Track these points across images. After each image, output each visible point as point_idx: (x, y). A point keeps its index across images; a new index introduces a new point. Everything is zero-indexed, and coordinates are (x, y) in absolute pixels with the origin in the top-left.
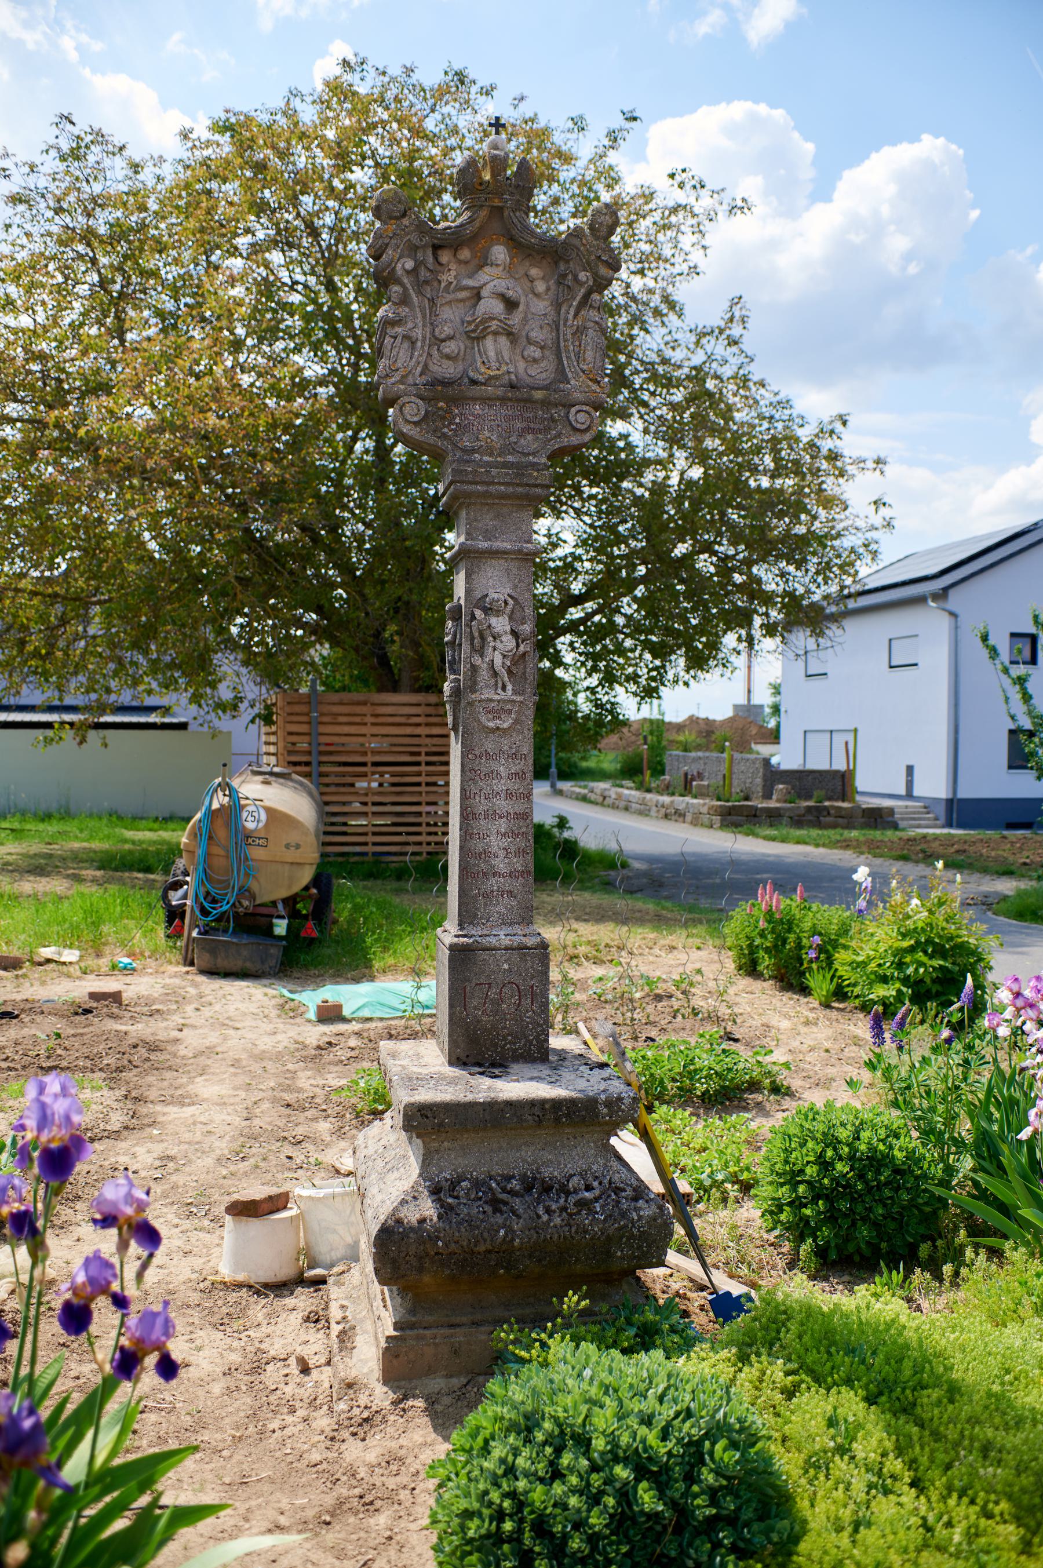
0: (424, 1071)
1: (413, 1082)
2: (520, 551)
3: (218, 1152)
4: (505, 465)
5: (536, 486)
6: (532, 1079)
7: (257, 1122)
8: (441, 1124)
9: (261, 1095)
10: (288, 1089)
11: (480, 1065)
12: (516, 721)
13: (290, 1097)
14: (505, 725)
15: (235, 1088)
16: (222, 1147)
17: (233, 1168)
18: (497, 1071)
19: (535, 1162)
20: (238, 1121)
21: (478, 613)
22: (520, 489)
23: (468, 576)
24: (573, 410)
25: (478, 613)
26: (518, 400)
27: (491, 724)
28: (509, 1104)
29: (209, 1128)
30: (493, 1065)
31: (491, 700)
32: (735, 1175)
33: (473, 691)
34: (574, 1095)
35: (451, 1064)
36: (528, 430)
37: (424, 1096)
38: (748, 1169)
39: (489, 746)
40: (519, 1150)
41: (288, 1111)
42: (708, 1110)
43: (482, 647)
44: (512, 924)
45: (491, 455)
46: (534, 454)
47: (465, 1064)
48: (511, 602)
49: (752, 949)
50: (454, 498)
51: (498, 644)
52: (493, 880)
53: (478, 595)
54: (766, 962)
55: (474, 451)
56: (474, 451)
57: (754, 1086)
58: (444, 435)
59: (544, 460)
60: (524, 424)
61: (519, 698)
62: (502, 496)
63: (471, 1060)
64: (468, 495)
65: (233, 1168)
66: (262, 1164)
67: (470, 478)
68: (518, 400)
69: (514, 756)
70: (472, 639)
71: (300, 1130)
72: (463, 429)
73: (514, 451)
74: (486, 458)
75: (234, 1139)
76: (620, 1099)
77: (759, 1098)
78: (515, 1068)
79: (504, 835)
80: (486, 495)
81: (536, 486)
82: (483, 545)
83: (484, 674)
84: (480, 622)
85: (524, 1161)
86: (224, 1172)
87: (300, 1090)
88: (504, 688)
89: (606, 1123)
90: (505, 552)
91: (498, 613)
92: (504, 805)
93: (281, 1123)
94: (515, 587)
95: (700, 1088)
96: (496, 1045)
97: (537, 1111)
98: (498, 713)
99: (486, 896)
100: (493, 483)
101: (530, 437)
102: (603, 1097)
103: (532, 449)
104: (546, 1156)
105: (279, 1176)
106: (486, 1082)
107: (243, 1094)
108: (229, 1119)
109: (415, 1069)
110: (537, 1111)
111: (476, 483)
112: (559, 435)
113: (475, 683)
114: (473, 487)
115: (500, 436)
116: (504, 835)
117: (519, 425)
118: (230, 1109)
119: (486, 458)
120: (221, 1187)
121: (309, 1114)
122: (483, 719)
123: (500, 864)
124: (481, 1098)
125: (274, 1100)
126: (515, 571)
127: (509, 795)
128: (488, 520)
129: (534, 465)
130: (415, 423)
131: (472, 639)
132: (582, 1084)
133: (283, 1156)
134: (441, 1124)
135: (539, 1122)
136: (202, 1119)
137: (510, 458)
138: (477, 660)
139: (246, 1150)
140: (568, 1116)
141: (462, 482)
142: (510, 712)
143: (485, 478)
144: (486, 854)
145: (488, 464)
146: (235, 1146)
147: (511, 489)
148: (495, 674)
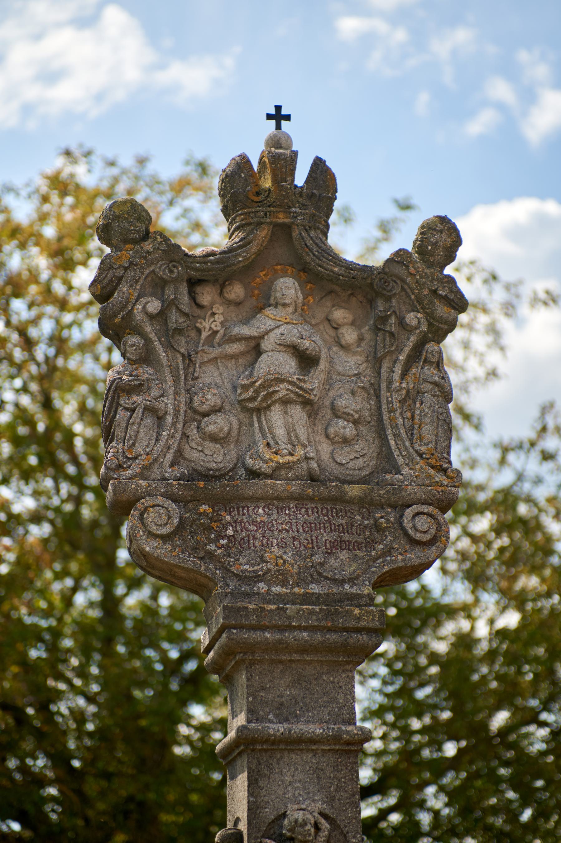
2: (337, 738)
4: (307, 599)
5: (358, 630)
22: (333, 637)
23: (252, 783)
24: (409, 512)
26: (323, 500)
36: (341, 544)
46: (352, 580)
48: (325, 825)
50: (227, 653)
53: (269, 814)
55: (256, 578)
56: (256, 578)
58: (210, 555)
59: (367, 590)
60: (334, 536)
62: (305, 649)
64: (250, 648)
67: (253, 620)
68: (323, 500)
72: (239, 544)
73: (319, 578)
74: (277, 589)
80: (279, 647)
81: (358, 630)
82: (277, 728)
90: (313, 741)
94: (330, 799)
100: (290, 628)
101: (344, 555)
103: (347, 573)
111: (264, 628)
112: (389, 551)
114: (257, 636)
115: (298, 554)
117: (325, 537)
119: (277, 589)
126: (329, 771)
128: (283, 688)
129: (352, 599)
130: (165, 538)
137: (314, 588)
141: (240, 627)
143: (277, 620)
145: (280, 598)
147: (318, 637)
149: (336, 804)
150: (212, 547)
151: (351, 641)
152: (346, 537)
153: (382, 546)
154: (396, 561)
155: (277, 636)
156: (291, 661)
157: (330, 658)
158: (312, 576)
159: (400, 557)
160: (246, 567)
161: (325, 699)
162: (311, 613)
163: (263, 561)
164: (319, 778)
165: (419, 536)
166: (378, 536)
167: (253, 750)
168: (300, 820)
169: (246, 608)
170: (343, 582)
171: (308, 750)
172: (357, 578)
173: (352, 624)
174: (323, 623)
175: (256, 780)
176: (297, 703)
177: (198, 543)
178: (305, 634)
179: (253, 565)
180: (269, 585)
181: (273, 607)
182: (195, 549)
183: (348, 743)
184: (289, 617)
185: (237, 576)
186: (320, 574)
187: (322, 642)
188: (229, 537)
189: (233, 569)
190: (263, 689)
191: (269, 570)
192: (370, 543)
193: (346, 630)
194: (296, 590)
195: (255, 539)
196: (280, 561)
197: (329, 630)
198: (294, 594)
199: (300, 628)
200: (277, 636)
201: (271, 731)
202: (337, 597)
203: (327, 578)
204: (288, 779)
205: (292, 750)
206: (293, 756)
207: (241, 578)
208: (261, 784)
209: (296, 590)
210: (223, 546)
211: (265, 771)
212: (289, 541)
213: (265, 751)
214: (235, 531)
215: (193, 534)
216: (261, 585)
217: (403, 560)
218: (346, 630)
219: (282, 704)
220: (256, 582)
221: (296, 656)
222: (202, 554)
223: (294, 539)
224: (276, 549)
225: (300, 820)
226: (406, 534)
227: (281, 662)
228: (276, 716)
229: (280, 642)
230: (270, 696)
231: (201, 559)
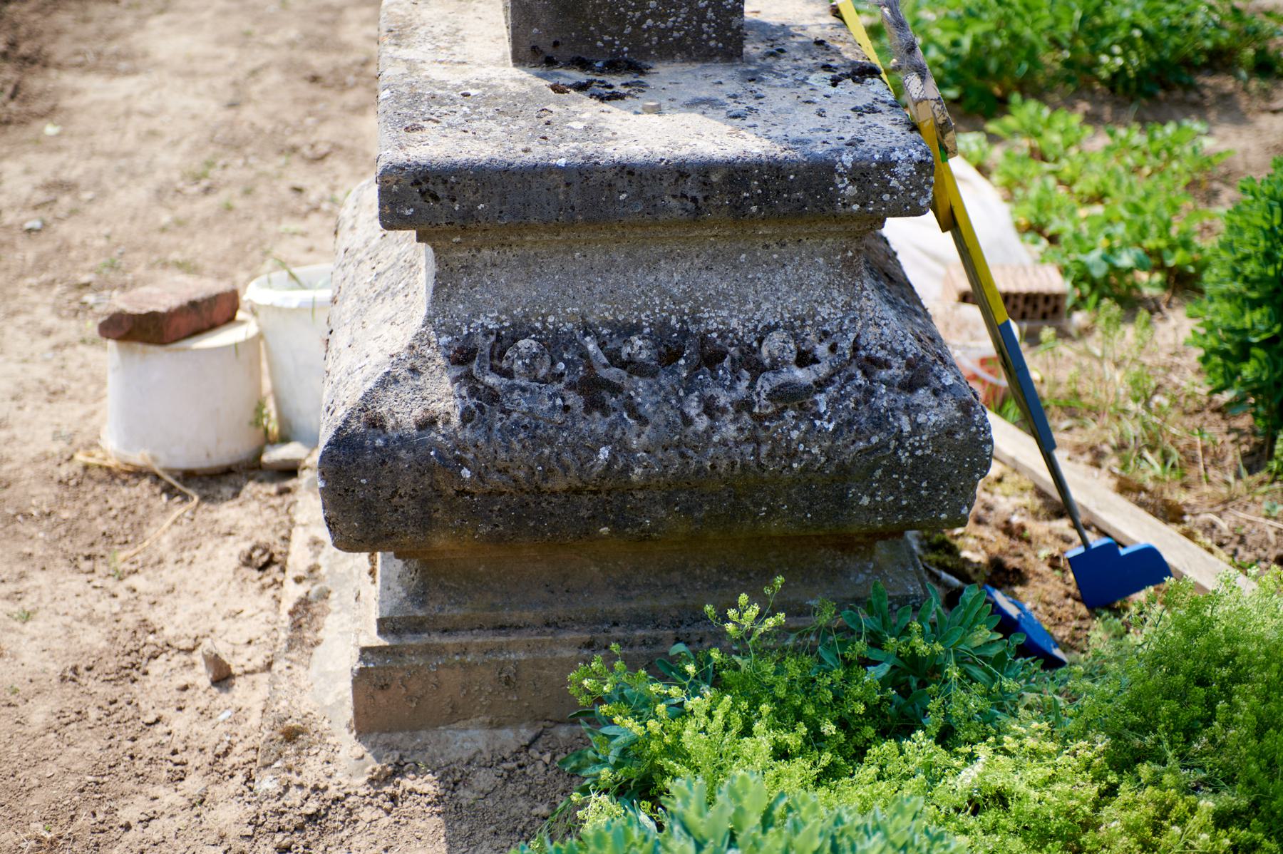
0: (454, 77)
1: (418, 106)
3: (160, 176)
6: (694, 104)
7: (248, 113)
8: (469, 215)
9: (264, 56)
10: (320, 44)
11: (582, 64)
13: (319, 62)
15: (221, 42)
16: (170, 162)
17: (183, 209)
18: (617, 82)
19: (688, 295)
20: (212, 110)
28: (627, 171)
29: (155, 124)
30: (614, 66)
32: (1156, 254)
34: (778, 151)
35: (519, 59)
37: (436, 147)
38: (1186, 245)
40: (652, 266)
41: (314, 91)
42: (1119, 106)
47: (550, 62)
57: (1220, 60)
63: (564, 52)
65: (183, 209)
66: (239, 203)
71: (327, 134)
75: (197, 148)
76: (887, 164)
77: (1229, 84)
78: (663, 73)
85: (664, 293)
86: (165, 218)
87: (343, 48)
89: (852, 217)
93: (291, 116)
95: (1110, 63)
96: (621, 20)
97: (691, 187)
102: (847, 159)
104: (716, 282)
105: (271, 228)
106: (587, 109)
107: (231, 54)
108: (196, 104)
109: (437, 73)
110: (691, 187)
118: (202, 85)
120: (154, 249)
121: (351, 98)
124: (561, 153)
125: (290, 68)
132: (804, 123)
133: (283, 188)
134: (469, 215)
135: (697, 214)
136: (145, 104)
139: (215, 173)
140: (762, 200)
146: (196, 165)
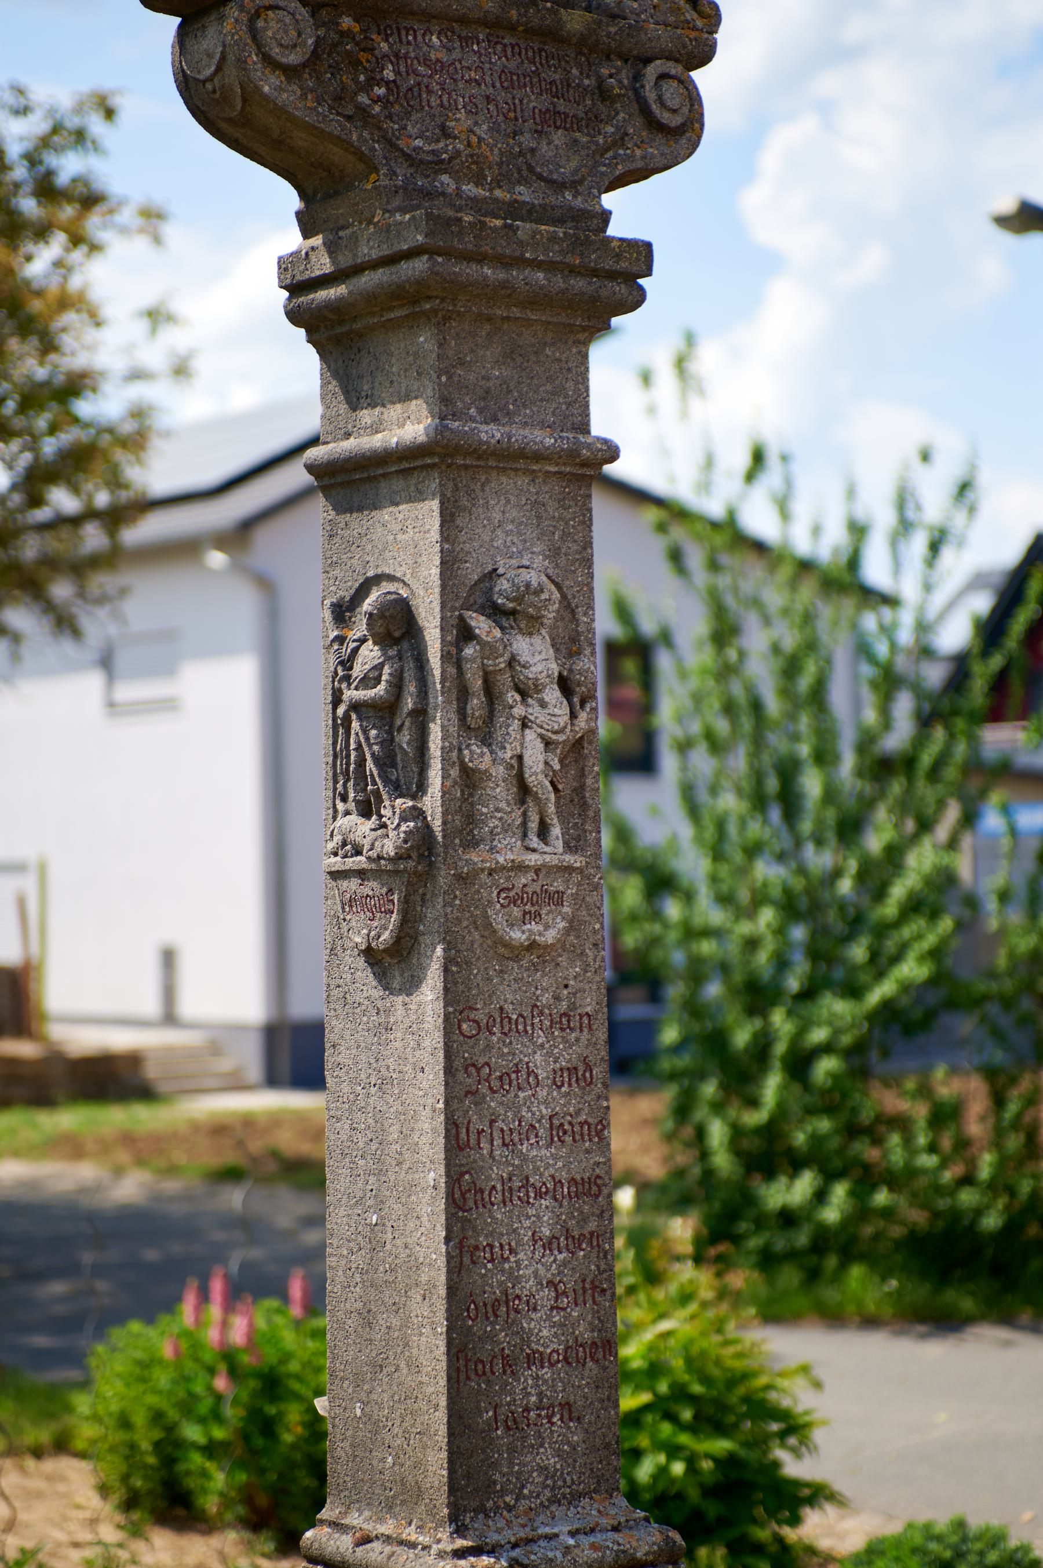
5: (612, 275)
12: (573, 926)
14: (550, 936)
21: (481, 624)
22: (579, 284)
24: (652, 71)
25: (481, 624)
26: (531, 32)
27: (517, 935)
31: (520, 868)
33: (472, 843)
36: (552, 119)
39: (509, 996)
43: (490, 718)
44: (575, 1498)
45: (479, 180)
49: (169, 1448)
51: (535, 712)
52: (528, 1375)
54: (216, 1483)
55: (438, 165)
56: (438, 165)
58: (363, 112)
61: (576, 860)
62: (537, 300)
67: (468, 243)
68: (531, 32)
69: (564, 1021)
70: (463, 694)
72: (404, 98)
73: (530, 174)
74: (469, 189)
79: (549, 1244)
80: (503, 292)
82: (490, 433)
83: (499, 793)
84: (489, 650)
88: (543, 832)
90: (538, 457)
91: (533, 624)
92: (547, 1160)
98: (533, 904)
99: (513, 1425)
100: (520, 262)
101: (559, 137)
111: (480, 258)
112: (621, 139)
113: (471, 819)
114: (471, 271)
116: (549, 1244)
117: (535, 102)
119: (469, 189)
122: (498, 919)
123: (543, 1331)
127: (557, 1131)
128: (490, 367)
130: (291, 72)
131: (463, 694)
137: (524, 194)
138: (479, 757)
141: (447, 253)
142: (557, 900)
144: (508, 1305)
145: (475, 204)
147: (559, 282)
148: (523, 791)
149: (562, 561)
150: (363, 99)
151: (604, 293)
152: (562, 106)
153: (610, 129)
154: (631, 158)
155: (502, 275)
156: (508, 318)
157: (563, 318)
158: (519, 171)
159: (638, 152)
160: (418, 143)
161: (549, 387)
162: (553, 238)
163: (445, 133)
164: (539, 517)
165: (666, 117)
166: (603, 109)
167: (449, 466)
168: (534, 584)
169: (460, 220)
170: (558, 186)
171: (527, 471)
172: (581, 182)
173: (608, 264)
174: (569, 259)
175: (452, 515)
176: (509, 392)
177: (344, 88)
178: (541, 275)
179: (429, 140)
180: (458, 181)
181: (498, 223)
182: (338, 98)
183: (584, 464)
184: (521, 243)
185: (407, 157)
186: (531, 169)
187: (563, 292)
188: (388, 83)
189: (401, 144)
190: (462, 363)
191: (458, 153)
192: (592, 121)
193: (595, 273)
194: (498, 193)
195: (429, 92)
196: (474, 139)
197: (573, 271)
198: (496, 200)
199: (536, 264)
200: (502, 275)
201: (484, 437)
202: (558, 213)
203: (541, 177)
204: (497, 516)
205: (504, 470)
206: (504, 479)
207: (411, 159)
208: (459, 522)
209: (498, 193)
210: (379, 99)
211: (465, 502)
212: (481, 104)
213: (466, 467)
214: (397, 73)
215: (335, 69)
216: (445, 178)
217: (644, 157)
218: (595, 273)
219: (488, 391)
220: (436, 172)
221: (516, 312)
222: (350, 110)
223: (488, 99)
224: (462, 115)
225: (534, 584)
226: (645, 111)
227: (489, 319)
228: (480, 411)
229: (504, 285)
230: (472, 377)
231: (349, 118)
